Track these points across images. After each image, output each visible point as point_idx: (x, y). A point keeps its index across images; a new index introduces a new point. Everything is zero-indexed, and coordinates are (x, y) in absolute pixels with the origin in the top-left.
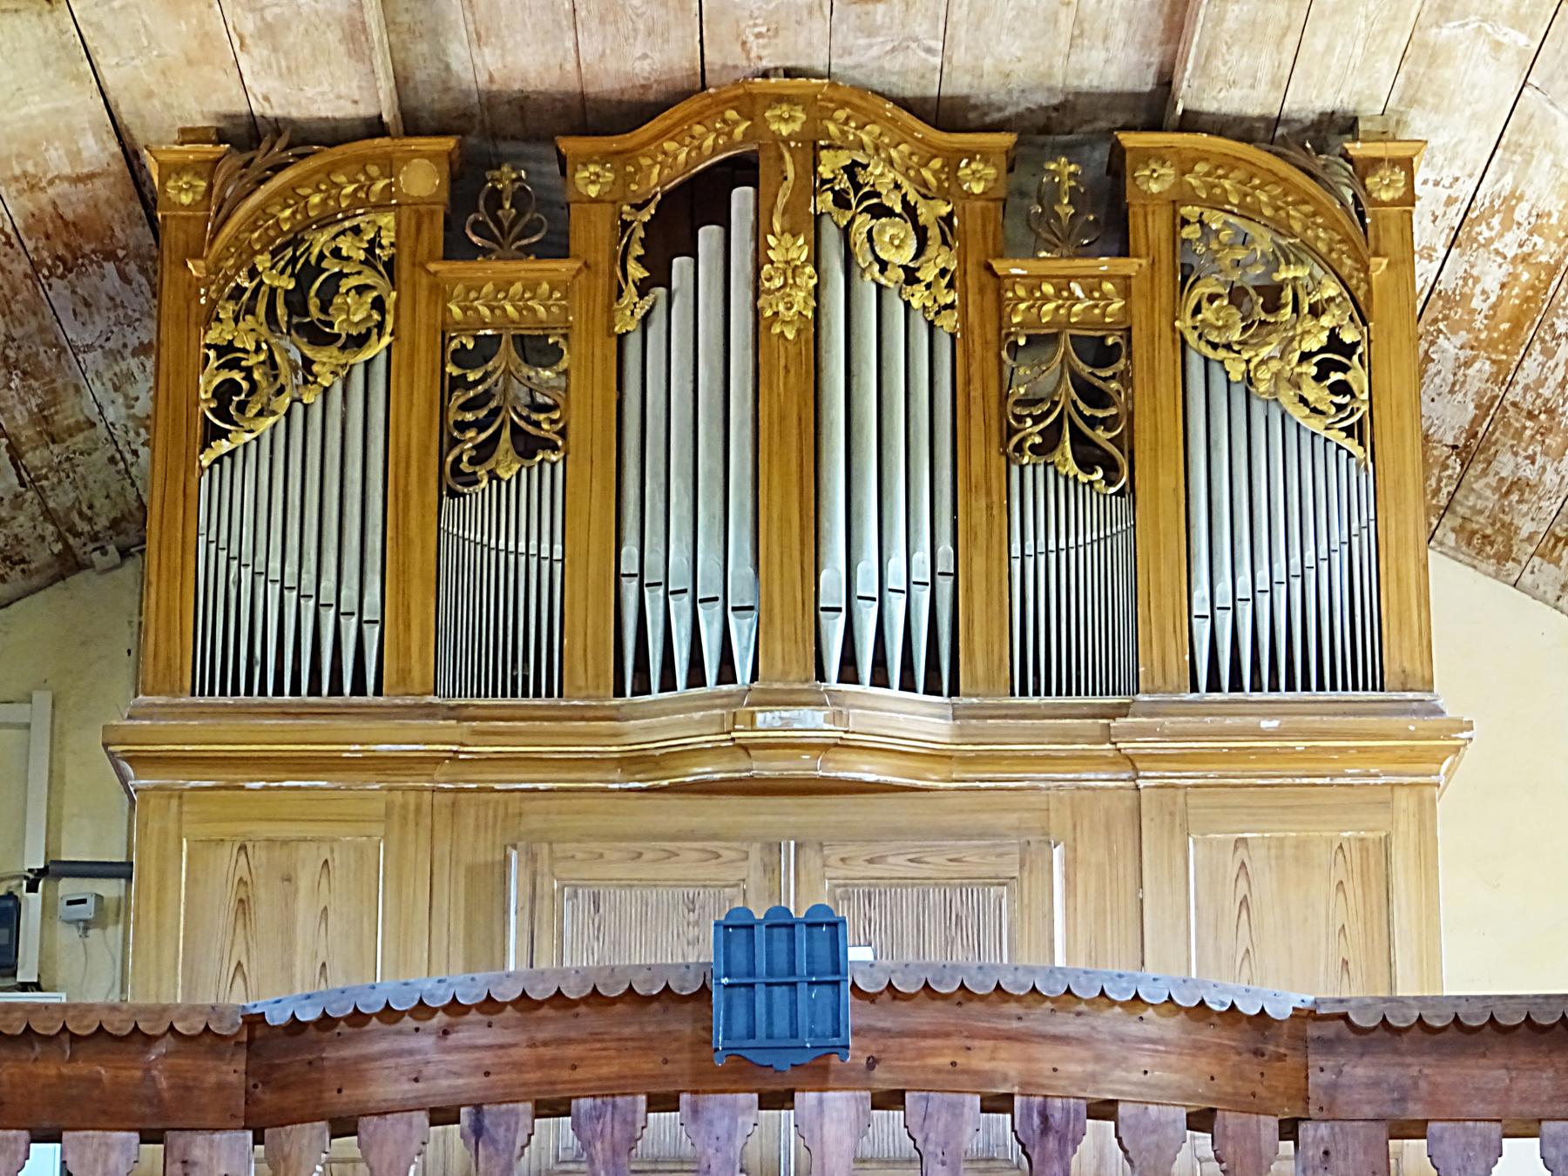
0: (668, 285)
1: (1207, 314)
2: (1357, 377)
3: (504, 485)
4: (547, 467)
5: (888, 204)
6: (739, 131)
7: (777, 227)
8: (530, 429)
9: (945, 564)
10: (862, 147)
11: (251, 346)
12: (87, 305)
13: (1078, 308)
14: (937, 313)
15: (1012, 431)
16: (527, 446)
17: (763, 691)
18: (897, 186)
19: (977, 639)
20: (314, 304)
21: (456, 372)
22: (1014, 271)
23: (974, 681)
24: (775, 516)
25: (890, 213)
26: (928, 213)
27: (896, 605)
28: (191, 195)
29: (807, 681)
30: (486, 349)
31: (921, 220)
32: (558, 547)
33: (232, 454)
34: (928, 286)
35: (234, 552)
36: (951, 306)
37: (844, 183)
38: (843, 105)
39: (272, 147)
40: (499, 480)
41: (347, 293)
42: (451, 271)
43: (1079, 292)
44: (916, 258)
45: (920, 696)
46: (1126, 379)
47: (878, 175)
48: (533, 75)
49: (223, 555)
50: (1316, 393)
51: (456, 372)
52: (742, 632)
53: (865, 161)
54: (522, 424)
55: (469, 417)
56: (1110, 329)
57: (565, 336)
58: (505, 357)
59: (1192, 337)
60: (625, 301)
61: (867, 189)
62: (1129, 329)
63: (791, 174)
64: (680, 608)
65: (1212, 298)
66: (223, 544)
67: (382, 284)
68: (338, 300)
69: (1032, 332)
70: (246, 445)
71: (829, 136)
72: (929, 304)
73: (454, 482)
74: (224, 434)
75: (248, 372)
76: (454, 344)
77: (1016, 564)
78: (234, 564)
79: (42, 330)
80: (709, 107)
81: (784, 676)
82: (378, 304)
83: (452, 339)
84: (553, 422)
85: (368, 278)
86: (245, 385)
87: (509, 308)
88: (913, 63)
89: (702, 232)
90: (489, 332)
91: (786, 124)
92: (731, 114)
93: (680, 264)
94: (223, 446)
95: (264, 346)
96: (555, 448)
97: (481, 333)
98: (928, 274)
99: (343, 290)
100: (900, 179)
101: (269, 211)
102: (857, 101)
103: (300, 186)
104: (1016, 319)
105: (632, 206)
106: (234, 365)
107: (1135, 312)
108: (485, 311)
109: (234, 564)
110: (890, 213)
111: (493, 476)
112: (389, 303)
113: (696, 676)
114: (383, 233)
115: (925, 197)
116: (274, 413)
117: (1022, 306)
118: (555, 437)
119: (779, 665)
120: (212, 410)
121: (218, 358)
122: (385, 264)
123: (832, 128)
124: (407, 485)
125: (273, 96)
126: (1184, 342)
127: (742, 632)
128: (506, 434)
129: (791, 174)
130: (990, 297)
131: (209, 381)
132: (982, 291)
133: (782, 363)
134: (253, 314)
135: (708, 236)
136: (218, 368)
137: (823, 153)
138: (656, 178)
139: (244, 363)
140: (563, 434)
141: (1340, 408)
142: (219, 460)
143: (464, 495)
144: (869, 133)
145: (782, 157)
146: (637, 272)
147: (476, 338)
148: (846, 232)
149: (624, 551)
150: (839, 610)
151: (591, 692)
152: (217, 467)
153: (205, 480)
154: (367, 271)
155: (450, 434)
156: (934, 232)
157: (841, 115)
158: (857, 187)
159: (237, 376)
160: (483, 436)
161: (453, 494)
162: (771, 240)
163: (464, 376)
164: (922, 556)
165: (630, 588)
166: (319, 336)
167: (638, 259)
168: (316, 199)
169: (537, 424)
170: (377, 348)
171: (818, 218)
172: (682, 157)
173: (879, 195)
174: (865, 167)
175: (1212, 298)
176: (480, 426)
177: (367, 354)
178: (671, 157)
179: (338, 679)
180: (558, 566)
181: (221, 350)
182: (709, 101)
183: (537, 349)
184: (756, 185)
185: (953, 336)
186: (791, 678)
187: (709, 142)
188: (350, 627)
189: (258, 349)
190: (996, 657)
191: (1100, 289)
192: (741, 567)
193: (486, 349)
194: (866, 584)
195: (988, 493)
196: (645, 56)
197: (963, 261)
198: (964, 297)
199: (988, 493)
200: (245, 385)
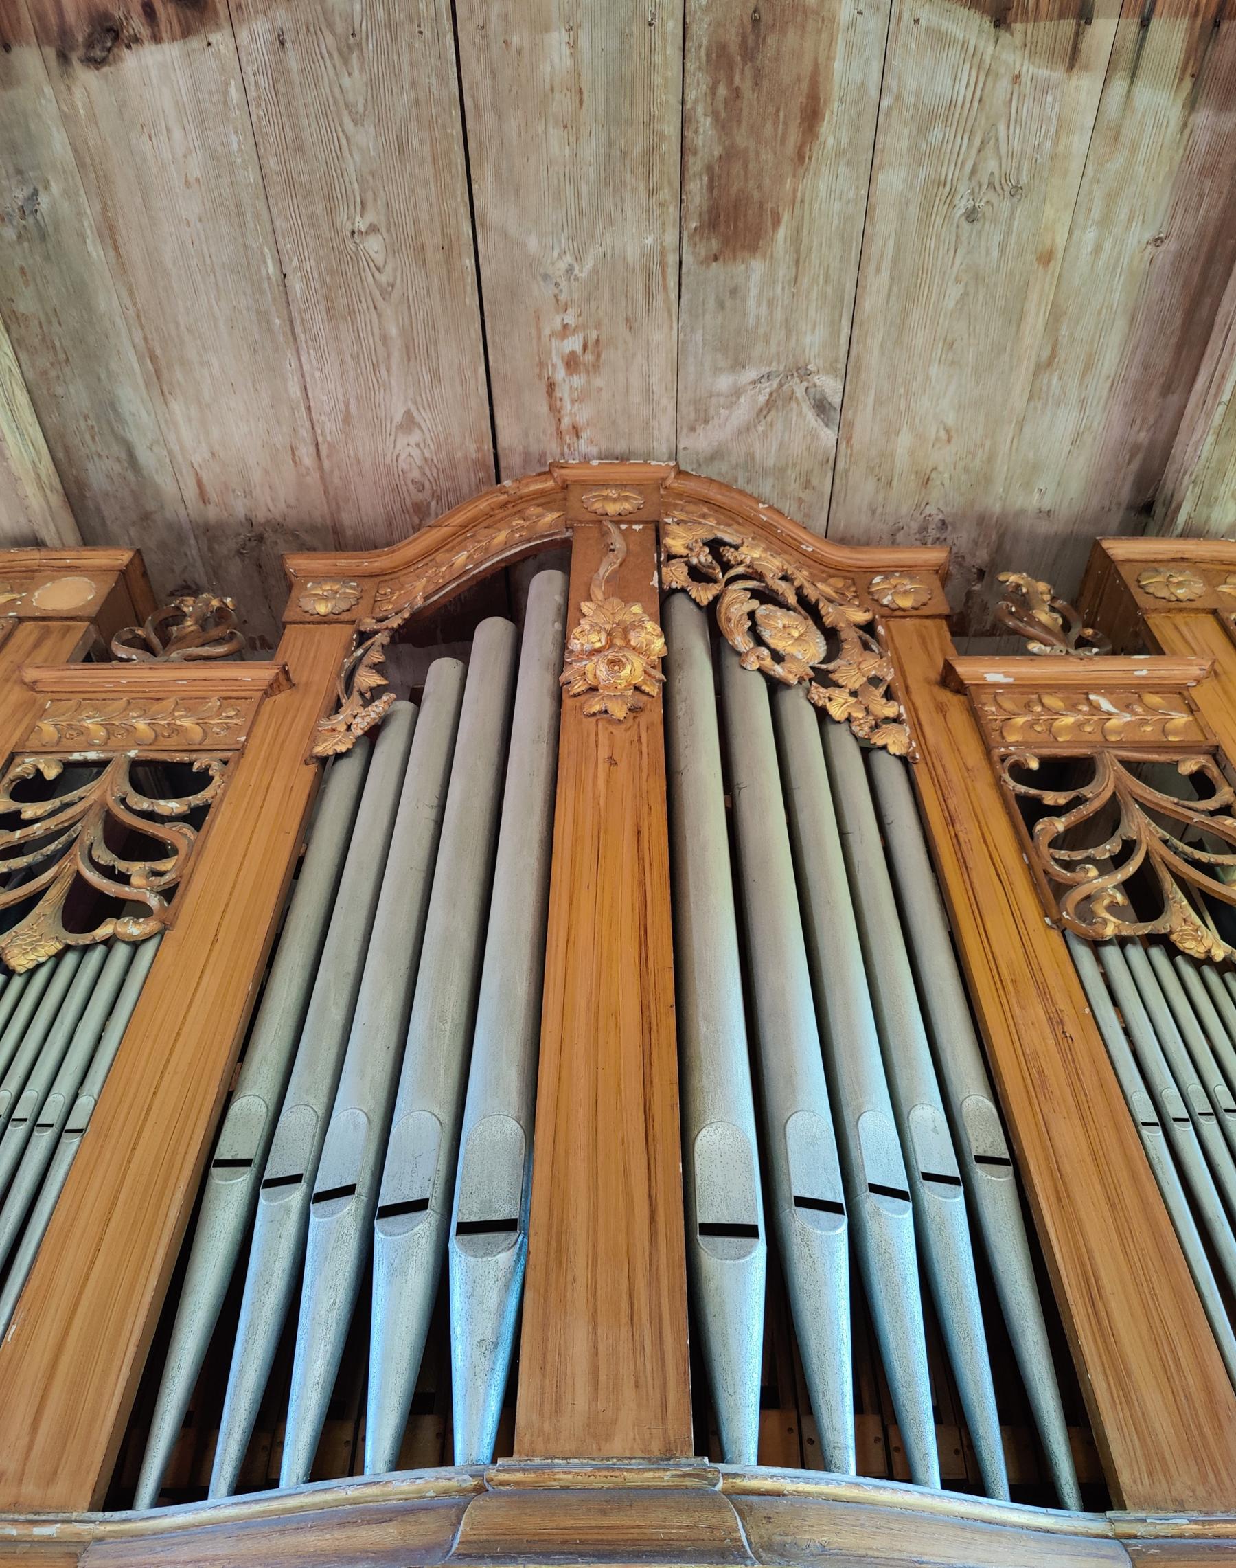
9: (985, 1136)
15: (1060, 890)
17: (523, 1494)
19: (1122, 1321)
22: (992, 677)
23: (1155, 1463)
27: (892, 1227)
29: (668, 1455)
30: (77, 773)
31: (828, 621)
34: (854, 694)
36: (896, 720)
37: (703, 557)
42: (59, 681)
45: (999, 1508)
48: (256, 476)
52: (483, 1286)
56: (1186, 749)
58: (109, 789)
61: (740, 570)
64: (337, 1227)
69: (1046, 752)
72: (859, 714)
77: (1155, 1138)
80: (503, 505)
81: (598, 1429)
88: (797, 447)
93: (442, 671)
117: (1020, 721)
119: (579, 1398)
127: (483, 1286)
133: (604, 753)
148: (711, 612)
150: (749, 1231)
151: (30, 1489)
162: (586, 607)
163: (19, 812)
164: (927, 1115)
165: (230, 1191)
169: (124, 879)
171: (666, 596)
182: (504, 497)
185: (905, 761)
186: (618, 1445)
190: (1193, 1381)
192: (493, 1124)
193: (77, 773)
194: (811, 1168)
195: (1044, 993)
196: (409, 423)
197: (901, 670)
199: (1044, 993)
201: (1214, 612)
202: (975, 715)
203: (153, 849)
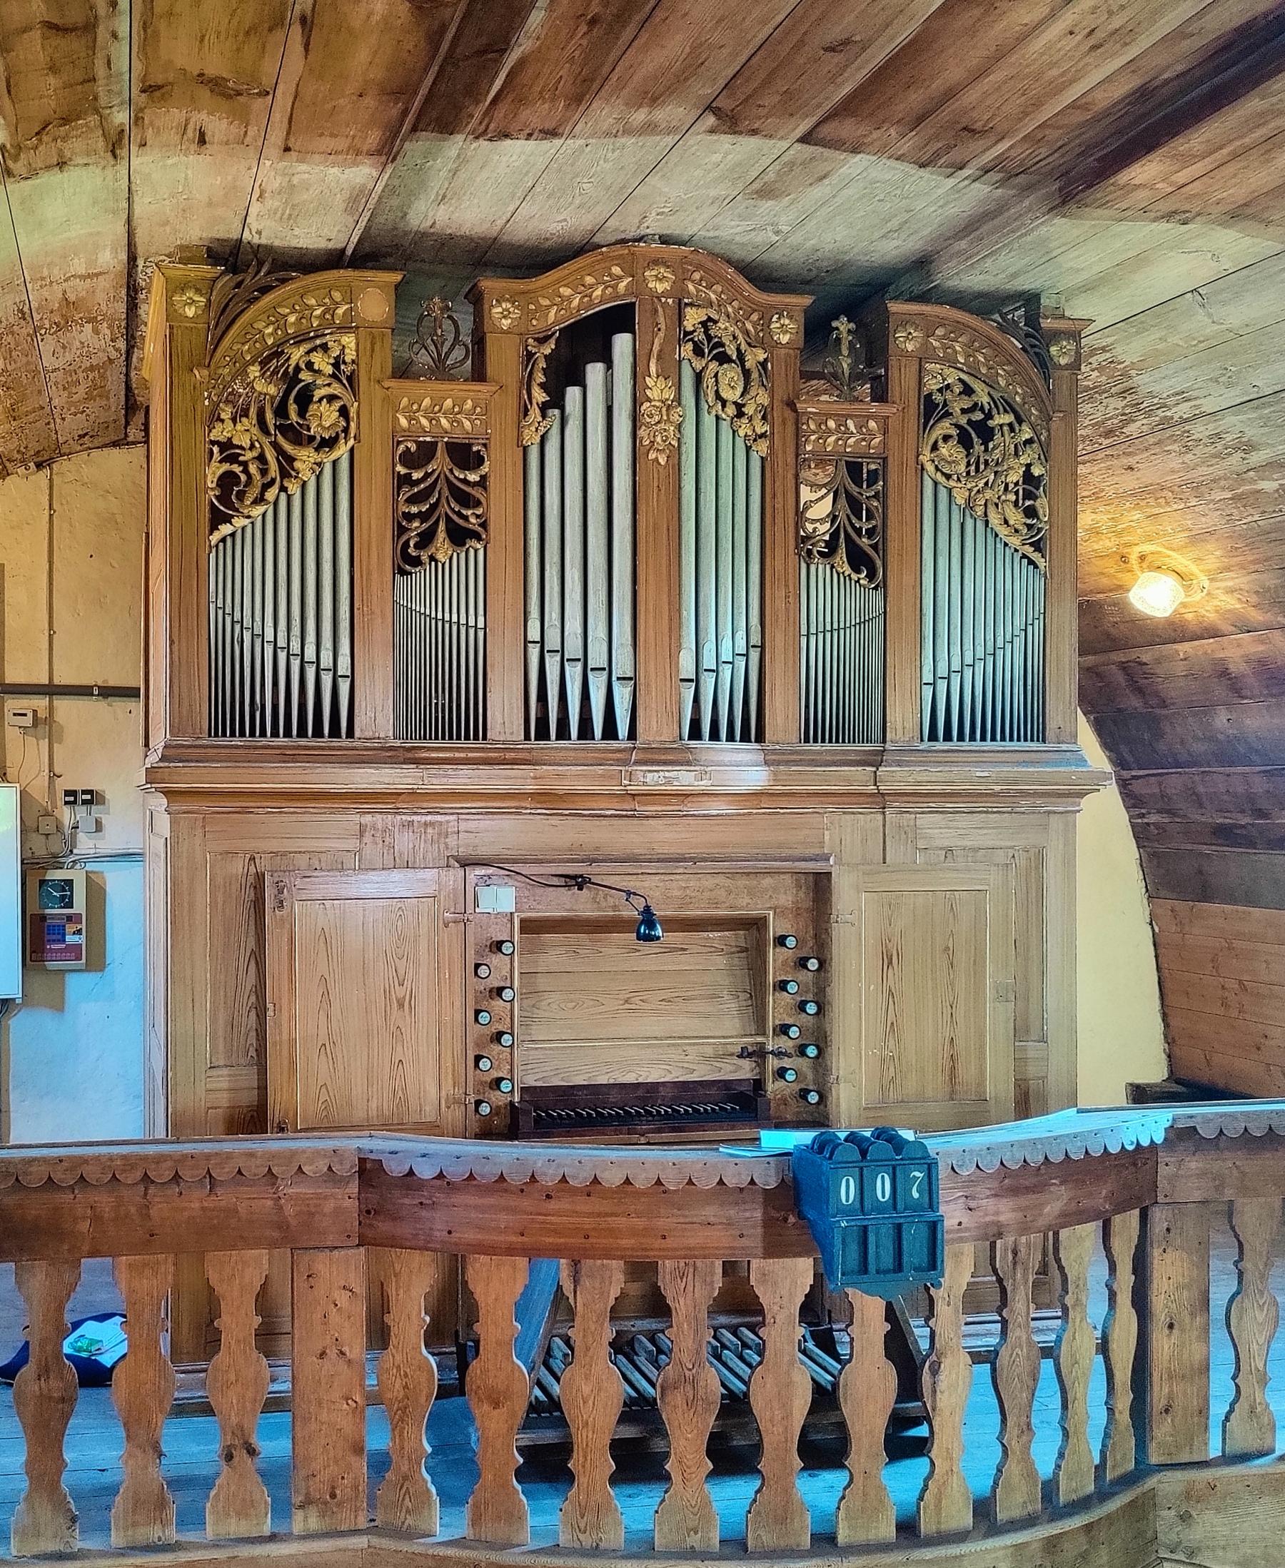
0: (562, 409)
1: (944, 450)
2: (1042, 504)
4: (472, 552)
5: (729, 353)
6: (622, 285)
8: (461, 522)
10: (711, 305)
11: (246, 444)
12: (64, 347)
13: (851, 441)
14: (755, 440)
16: (459, 536)
18: (735, 337)
20: (293, 409)
25: (730, 360)
26: (755, 357)
28: (193, 309)
31: (748, 365)
33: (233, 535)
35: (237, 616)
36: (763, 436)
37: (700, 336)
38: (699, 267)
39: (258, 272)
40: (436, 561)
41: (320, 400)
43: (852, 428)
44: (742, 395)
46: (882, 497)
47: (724, 329)
49: (228, 619)
50: (1016, 517)
51: (401, 470)
53: (716, 317)
54: (455, 517)
55: (414, 510)
57: (485, 445)
58: (440, 463)
59: (930, 468)
60: (530, 418)
62: (885, 459)
63: (663, 326)
64: (574, 674)
65: (946, 438)
66: (228, 610)
67: (347, 398)
68: (313, 407)
70: (243, 529)
71: (689, 295)
73: (406, 562)
74: (228, 519)
75: (245, 465)
76: (402, 447)
78: (238, 627)
79: (28, 363)
82: (344, 412)
83: (399, 443)
84: (478, 517)
85: (336, 389)
86: (243, 477)
87: (443, 421)
89: (589, 367)
90: (428, 439)
91: (659, 283)
92: (616, 270)
94: (225, 529)
95: (257, 445)
96: (479, 539)
98: (749, 410)
99: (315, 399)
100: (737, 332)
101: (255, 326)
102: (709, 265)
103: (280, 306)
104: (809, 448)
105: (535, 339)
106: (233, 459)
107: (891, 444)
108: (424, 422)
109: (238, 627)
110: (730, 360)
112: (352, 413)
114: (347, 351)
115: (749, 344)
117: (813, 438)
118: (480, 529)
120: (217, 497)
121: (221, 452)
122: (350, 379)
123: (691, 287)
125: (266, 228)
126: (923, 469)
128: (442, 526)
129: (663, 326)
130: (790, 429)
131: (215, 470)
132: (784, 422)
134: (247, 416)
135: (595, 372)
136: (220, 462)
137: (688, 309)
138: (554, 318)
139: (241, 458)
140: (484, 525)
141: (1030, 527)
142: (223, 540)
143: (411, 574)
144: (715, 292)
145: (656, 311)
146: (540, 396)
147: (415, 442)
149: (529, 623)
152: (221, 545)
153: (213, 555)
154: (335, 385)
155: (399, 523)
156: (755, 375)
157: (697, 276)
158: (709, 338)
159: (237, 469)
160: (425, 526)
161: (403, 573)
166: (298, 437)
168: (292, 319)
169: (466, 518)
170: (342, 450)
172: (576, 303)
173: (723, 345)
174: (715, 322)
175: (946, 438)
176: (423, 517)
177: (334, 456)
178: (569, 297)
180: (481, 634)
181: (226, 446)
183: (465, 455)
184: (633, 333)
187: (598, 292)
188: (327, 680)
189: (252, 447)
191: (867, 427)
193: (426, 452)
198: (772, 427)
200: (243, 477)
202: (797, 423)
203: (473, 503)
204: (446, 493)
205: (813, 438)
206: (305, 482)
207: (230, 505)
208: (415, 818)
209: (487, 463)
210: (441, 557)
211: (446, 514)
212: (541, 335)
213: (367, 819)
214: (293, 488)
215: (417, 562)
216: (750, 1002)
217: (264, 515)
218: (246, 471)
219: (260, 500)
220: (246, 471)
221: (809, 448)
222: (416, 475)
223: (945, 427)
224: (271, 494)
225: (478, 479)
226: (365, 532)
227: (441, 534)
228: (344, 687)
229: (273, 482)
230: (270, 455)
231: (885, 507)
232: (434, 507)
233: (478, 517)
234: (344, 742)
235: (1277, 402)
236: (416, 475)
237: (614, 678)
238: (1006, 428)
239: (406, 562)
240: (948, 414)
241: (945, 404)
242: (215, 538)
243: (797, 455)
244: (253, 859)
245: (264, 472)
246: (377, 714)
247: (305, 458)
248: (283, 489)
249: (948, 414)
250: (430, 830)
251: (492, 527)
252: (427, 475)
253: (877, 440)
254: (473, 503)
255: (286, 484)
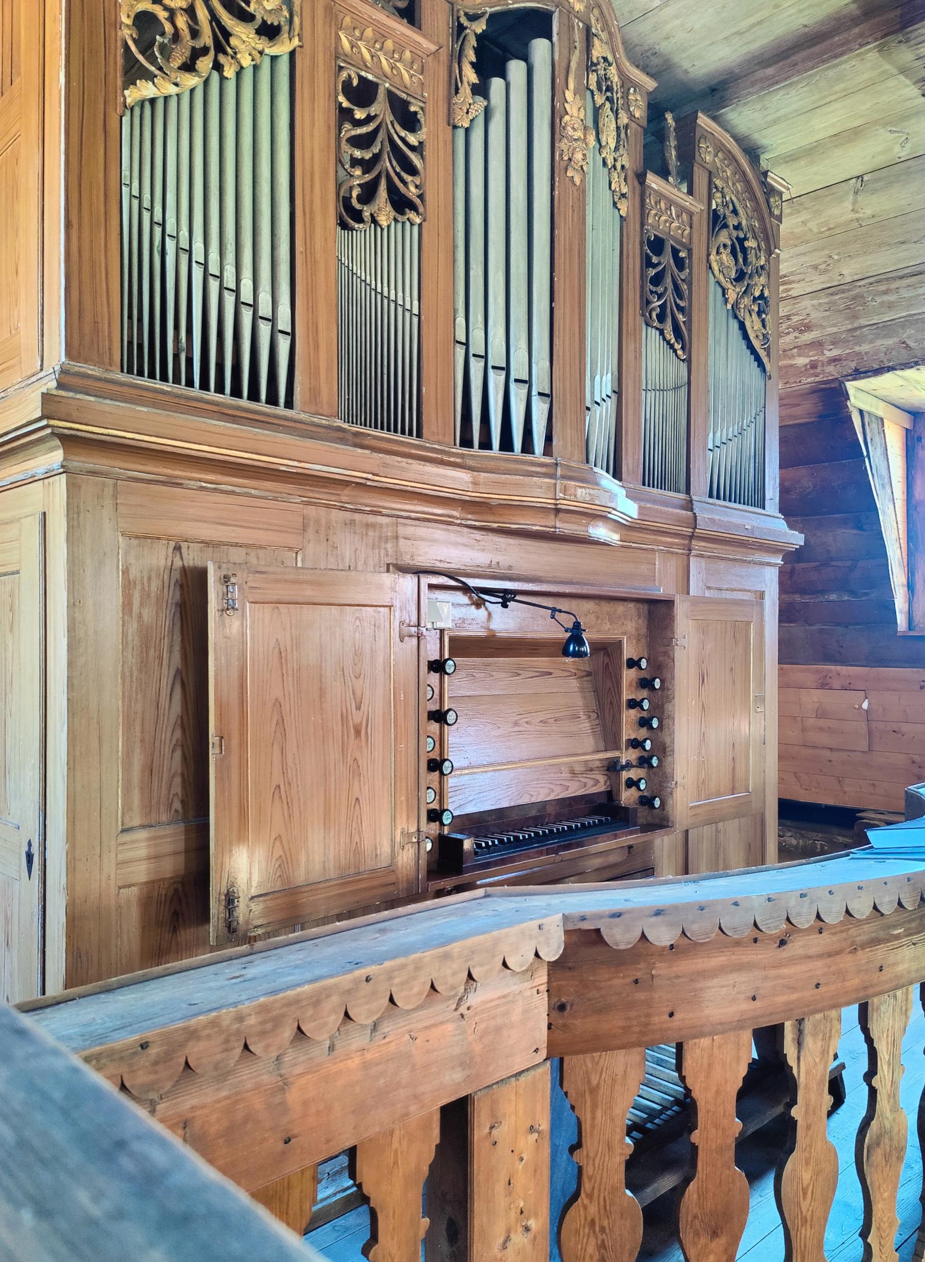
2: (768, 318)
3: (379, 229)
7: (571, 85)
21: (346, 104)
24: (567, 326)
32: (416, 303)
51: (346, 104)
57: (422, 108)
64: (496, 381)
73: (349, 216)
74: (151, 77)
76: (344, 75)
86: (168, 27)
90: (370, 77)
93: (497, 83)
94: (146, 89)
97: (363, 74)
105: (466, 14)
111: (374, 221)
113: (507, 444)
116: (200, 77)
124: (312, 203)
129: (577, 44)
140: (421, 197)
142: (142, 103)
143: (352, 229)
146: (471, 76)
160: (368, 177)
161: (344, 226)
167: (472, 63)
170: (282, 48)
179: (255, 384)
180: (415, 320)
184: (551, 41)
200: (168, 27)
201: (710, 172)
204: (388, 148)
205: (653, 212)
206: (242, 68)
207: (152, 60)
208: (357, 516)
209: (424, 130)
210: (383, 220)
211: (387, 170)
212: (471, 12)
213: (311, 511)
214: (229, 72)
215: (358, 217)
216: (597, 722)
217: (192, 91)
218: (172, 20)
219: (189, 67)
220: (172, 20)
221: (650, 221)
222: (359, 114)
223: (724, 237)
224: (205, 64)
225: (416, 144)
226: (308, 162)
227: (382, 192)
228: (284, 344)
229: (205, 51)
230: (202, 14)
231: (690, 289)
232: (376, 158)
233: (417, 187)
234: (281, 410)
235: (849, 290)
236: (359, 114)
237: (534, 393)
238: (753, 251)
239: (349, 216)
240: (725, 226)
241: (724, 218)
242: (132, 95)
243: (642, 225)
244: (178, 548)
245: (195, 34)
246: (320, 382)
247: (244, 37)
248: (218, 67)
249: (725, 226)
250: (371, 533)
251: (428, 197)
252: (369, 119)
253: (687, 232)
254: (413, 171)
255: (222, 59)
